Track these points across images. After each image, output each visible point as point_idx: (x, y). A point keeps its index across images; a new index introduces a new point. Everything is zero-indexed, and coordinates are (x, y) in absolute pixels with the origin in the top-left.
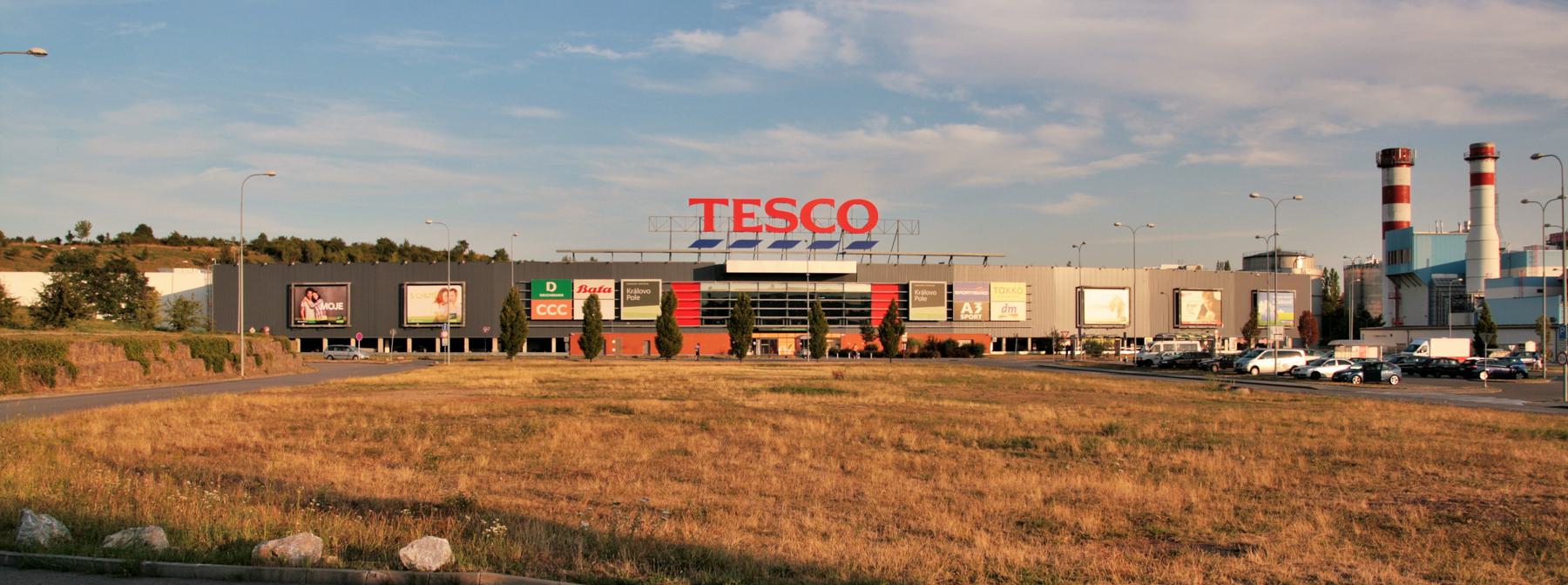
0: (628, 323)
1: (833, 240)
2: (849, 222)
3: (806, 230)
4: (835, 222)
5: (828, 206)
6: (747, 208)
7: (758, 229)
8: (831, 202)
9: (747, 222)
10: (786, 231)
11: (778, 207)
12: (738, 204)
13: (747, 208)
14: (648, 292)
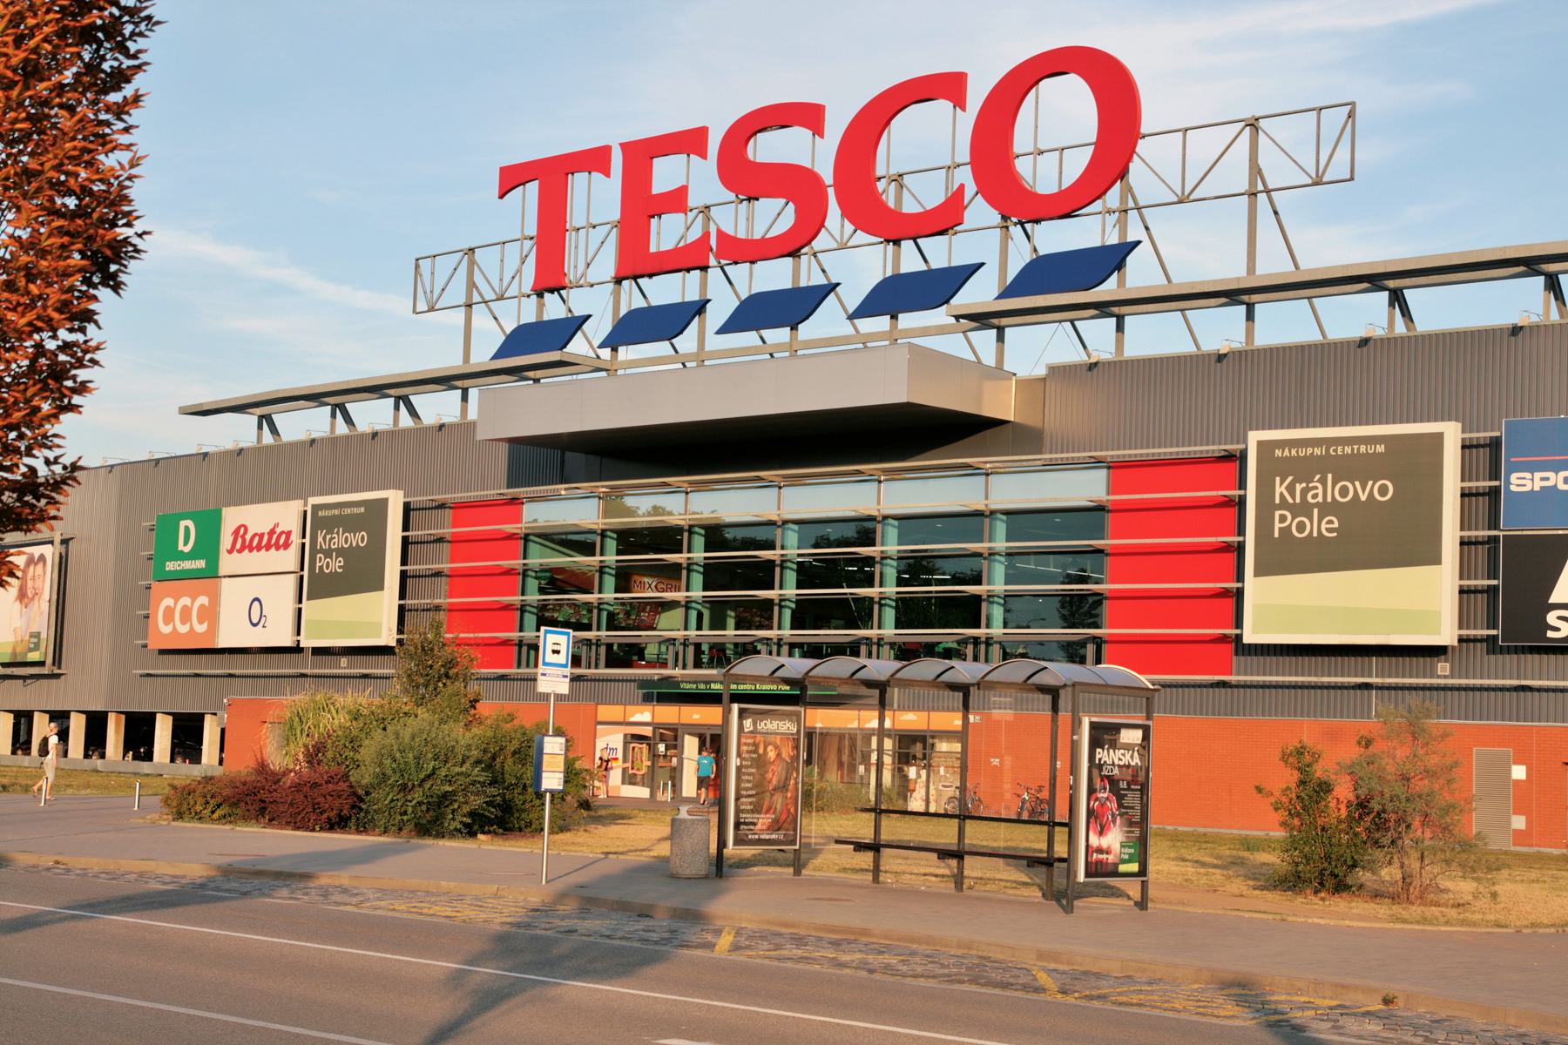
0: (344, 661)
1: (957, 261)
2: (1023, 167)
3: (862, 237)
4: (965, 176)
5: (942, 106)
6: (666, 173)
7: (689, 259)
8: (950, 87)
9: (667, 233)
10: (792, 246)
11: (770, 148)
12: (642, 154)
13: (666, 173)
14: (359, 539)
